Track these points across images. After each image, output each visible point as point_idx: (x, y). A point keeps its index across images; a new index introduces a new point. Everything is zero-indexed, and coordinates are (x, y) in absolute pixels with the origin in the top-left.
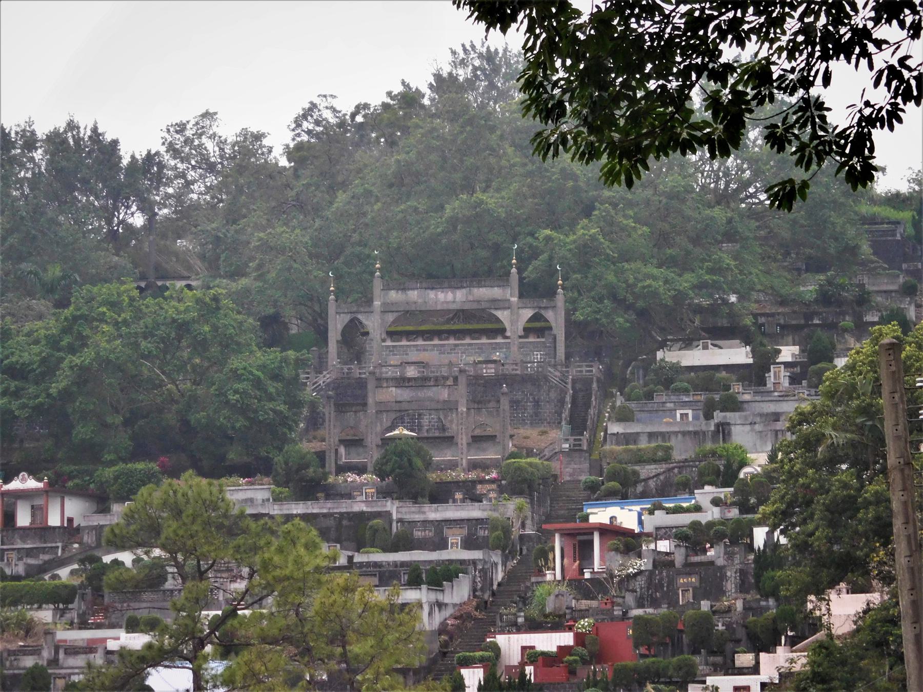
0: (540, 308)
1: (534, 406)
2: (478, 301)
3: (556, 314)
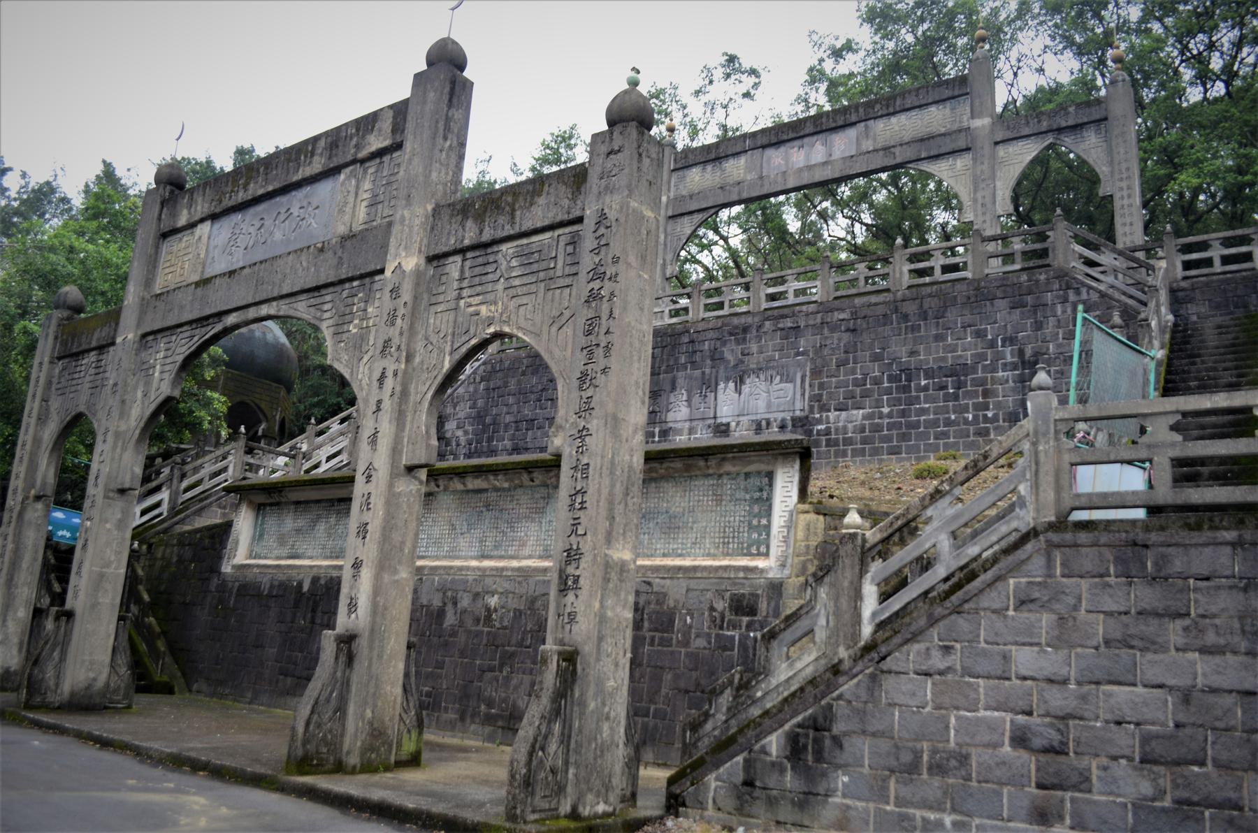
0: (1060, 130)
2: (886, 149)
3: (1107, 140)
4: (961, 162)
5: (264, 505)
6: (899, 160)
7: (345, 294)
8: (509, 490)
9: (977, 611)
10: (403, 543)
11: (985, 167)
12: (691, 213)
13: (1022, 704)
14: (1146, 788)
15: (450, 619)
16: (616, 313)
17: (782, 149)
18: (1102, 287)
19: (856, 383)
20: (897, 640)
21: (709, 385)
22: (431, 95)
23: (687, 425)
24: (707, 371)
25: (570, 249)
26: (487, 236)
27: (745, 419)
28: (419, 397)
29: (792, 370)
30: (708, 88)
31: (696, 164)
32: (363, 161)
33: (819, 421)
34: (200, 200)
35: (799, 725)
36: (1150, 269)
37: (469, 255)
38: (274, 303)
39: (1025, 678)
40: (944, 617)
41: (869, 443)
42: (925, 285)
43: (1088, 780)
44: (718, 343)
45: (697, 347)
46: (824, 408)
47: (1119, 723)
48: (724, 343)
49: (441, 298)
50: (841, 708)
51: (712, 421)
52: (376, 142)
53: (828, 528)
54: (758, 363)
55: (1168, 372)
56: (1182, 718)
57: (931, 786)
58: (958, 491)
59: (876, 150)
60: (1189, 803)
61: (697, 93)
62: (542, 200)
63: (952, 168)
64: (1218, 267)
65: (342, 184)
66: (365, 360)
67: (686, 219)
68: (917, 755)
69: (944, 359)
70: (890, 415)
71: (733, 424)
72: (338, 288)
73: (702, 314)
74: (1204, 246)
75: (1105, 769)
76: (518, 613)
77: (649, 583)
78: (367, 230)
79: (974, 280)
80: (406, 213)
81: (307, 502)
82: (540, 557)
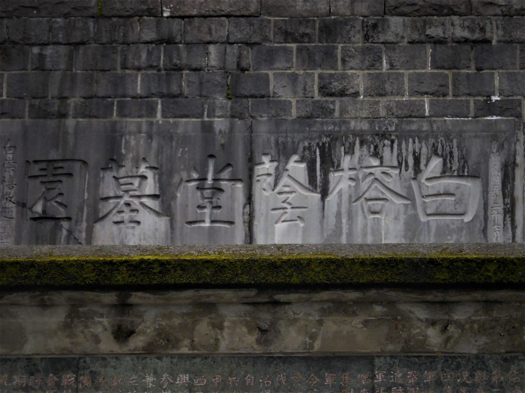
8: (479, 362)
24: (220, 124)
29: (475, 148)
44: (249, 57)
45: (184, 56)
48: (269, 58)
54: (373, 119)
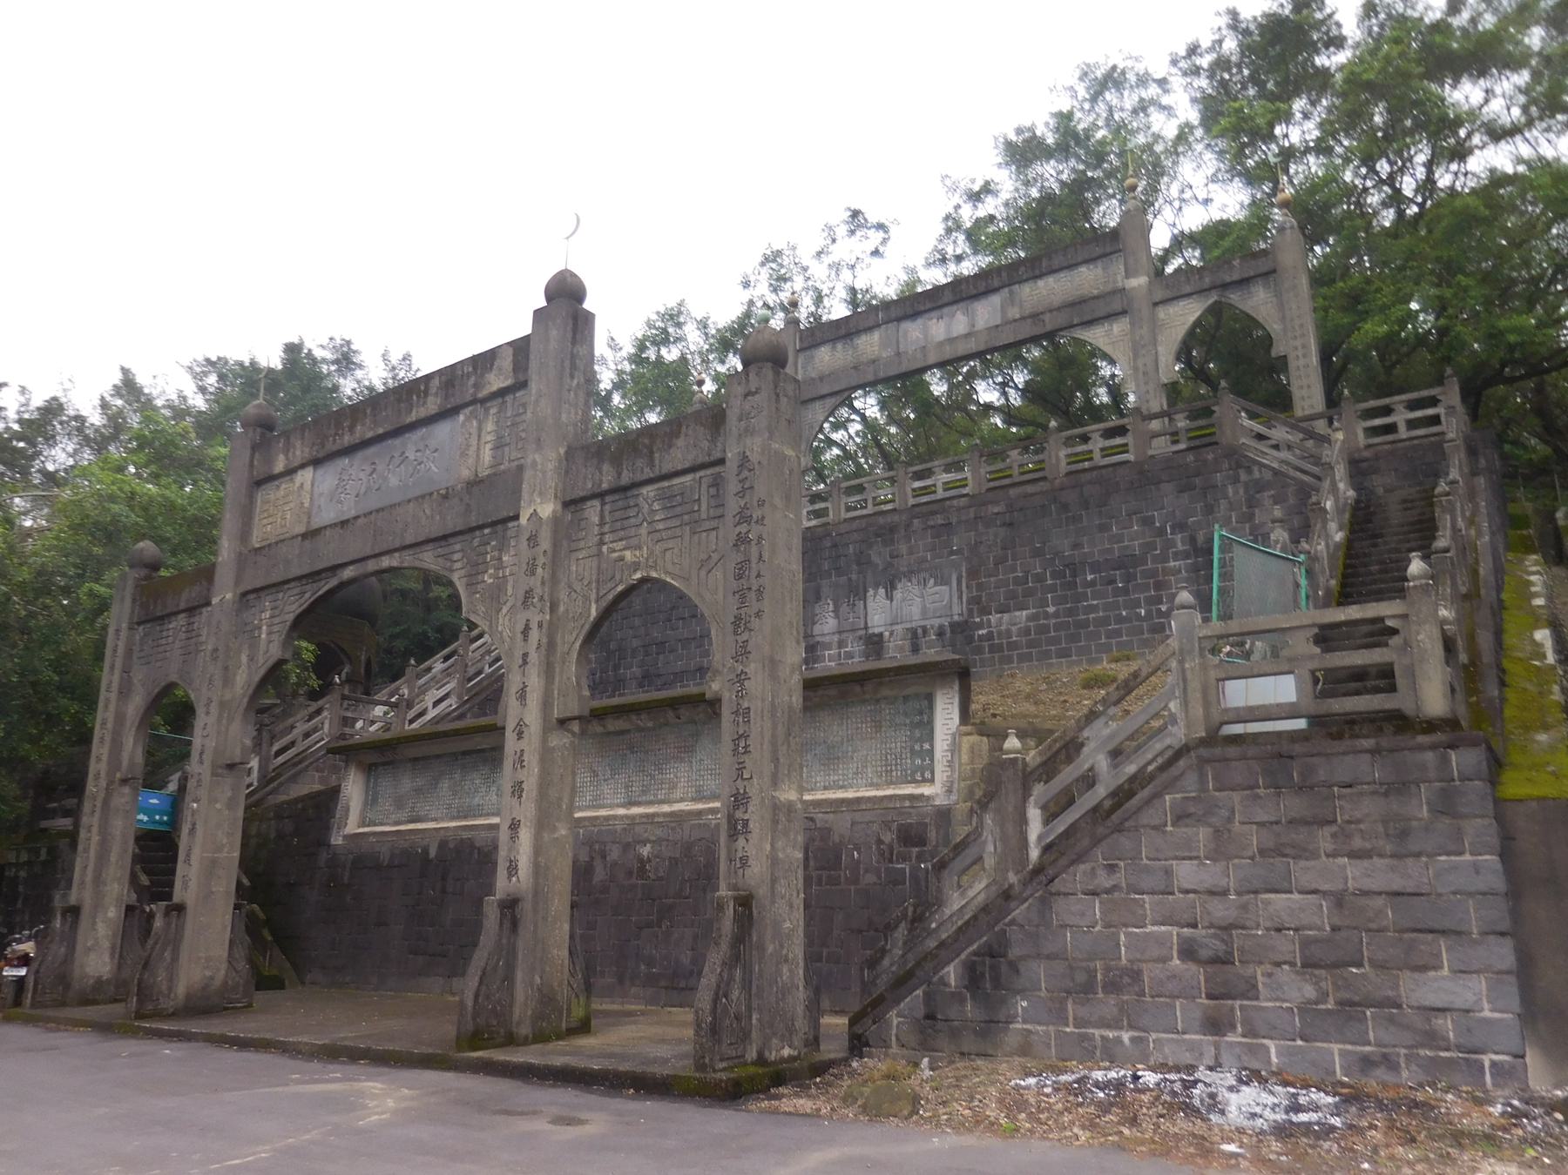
0: (1225, 286)
1: (1195, 569)
3: (1278, 295)
4: (1119, 327)
5: (376, 765)
6: (1049, 327)
7: (476, 542)
9: (1136, 828)
10: (560, 799)
11: (1145, 331)
12: (823, 397)
13: (1186, 917)
14: (1309, 992)
15: (600, 874)
16: (766, 556)
17: (920, 321)
18: (1275, 465)
19: (1017, 581)
20: (1063, 861)
21: (857, 592)
22: (554, 333)
23: (836, 638)
24: (854, 577)
25: (713, 491)
26: (626, 479)
27: (899, 627)
28: (566, 648)
30: (832, 248)
31: (823, 343)
32: (483, 401)
33: (980, 626)
34: (298, 444)
35: (975, 953)
36: (1325, 440)
37: (608, 499)
38: (397, 555)
39: (1187, 892)
40: (1106, 837)
41: (1039, 646)
42: (1085, 470)
43: (1255, 987)
46: (985, 611)
47: (1279, 930)
49: (582, 544)
50: (1014, 934)
51: (862, 632)
52: (496, 382)
53: (992, 749)
55: (1348, 556)
56: (1337, 921)
57: (1108, 1005)
58: (1112, 711)
59: (1023, 318)
60: (1352, 1004)
61: (819, 254)
62: (680, 442)
63: (1108, 334)
64: (1403, 433)
65: (463, 425)
66: (505, 610)
67: (818, 404)
68: (1092, 974)
69: (1110, 551)
70: (1056, 615)
71: (887, 634)
72: (467, 537)
73: (844, 515)
74: (1387, 411)
75: (1270, 975)
76: (674, 862)
77: (812, 819)
78: (495, 474)
79: (1136, 462)
80: (537, 457)
81: (424, 758)
82: (693, 800)
